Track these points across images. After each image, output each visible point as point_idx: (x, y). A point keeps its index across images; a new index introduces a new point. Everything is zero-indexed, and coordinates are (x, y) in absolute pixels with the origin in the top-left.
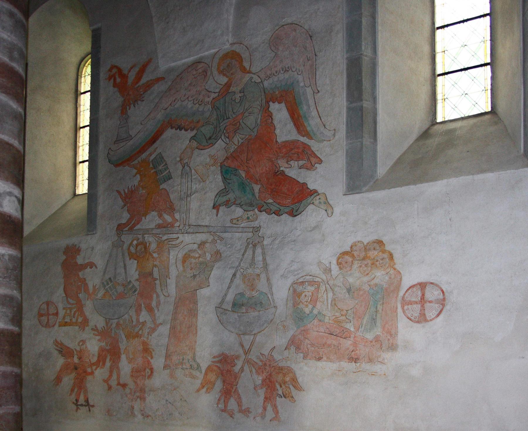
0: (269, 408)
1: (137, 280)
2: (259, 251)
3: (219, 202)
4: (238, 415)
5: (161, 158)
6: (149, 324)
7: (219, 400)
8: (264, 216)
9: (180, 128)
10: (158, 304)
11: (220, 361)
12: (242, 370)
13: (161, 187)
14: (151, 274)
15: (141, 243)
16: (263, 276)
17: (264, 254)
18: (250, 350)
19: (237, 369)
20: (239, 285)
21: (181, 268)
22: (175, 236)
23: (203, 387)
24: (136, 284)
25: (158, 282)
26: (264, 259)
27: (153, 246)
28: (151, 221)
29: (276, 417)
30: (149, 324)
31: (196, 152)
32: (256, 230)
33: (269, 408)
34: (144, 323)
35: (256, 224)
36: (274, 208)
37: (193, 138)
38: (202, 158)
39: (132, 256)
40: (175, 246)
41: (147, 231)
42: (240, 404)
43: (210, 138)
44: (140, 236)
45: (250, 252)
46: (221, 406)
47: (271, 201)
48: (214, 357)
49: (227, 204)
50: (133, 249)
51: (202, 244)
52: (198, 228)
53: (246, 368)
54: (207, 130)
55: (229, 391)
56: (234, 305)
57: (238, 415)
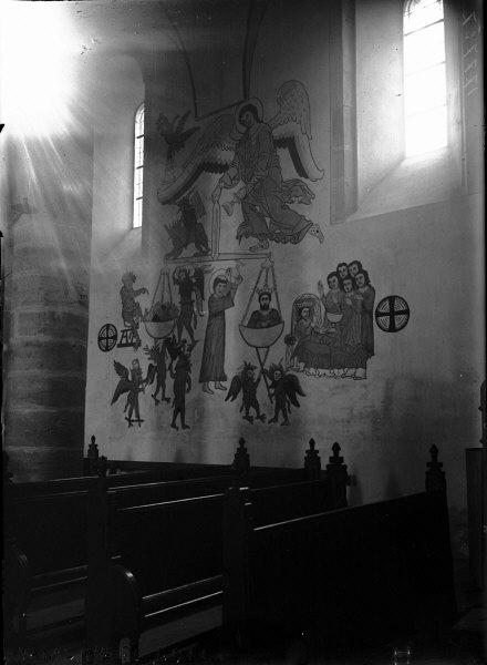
12: (259, 380)
25: (195, 304)
26: (275, 281)
28: (190, 250)
30: (189, 342)
32: (269, 255)
34: (185, 341)
38: (227, 196)
50: (177, 277)
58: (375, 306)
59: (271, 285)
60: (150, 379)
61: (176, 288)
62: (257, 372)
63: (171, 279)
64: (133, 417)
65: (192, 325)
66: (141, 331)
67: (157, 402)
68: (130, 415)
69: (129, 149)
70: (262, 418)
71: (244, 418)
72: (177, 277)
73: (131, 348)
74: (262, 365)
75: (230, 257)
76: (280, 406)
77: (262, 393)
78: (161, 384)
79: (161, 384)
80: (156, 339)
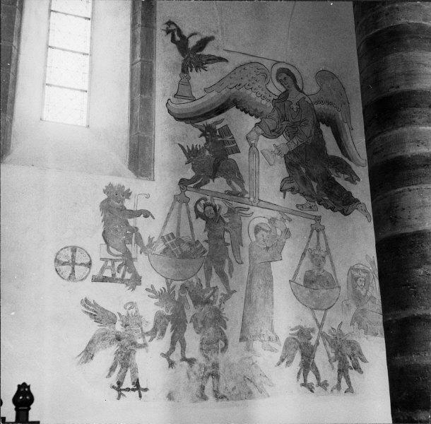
0: (343, 380)
1: (206, 241)
2: (321, 235)
3: (284, 188)
4: (317, 389)
6: (222, 290)
7: (299, 374)
8: (322, 208)
11: (298, 334)
12: (318, 343)
14: (222, 238)
16: (327, 259)
17: (326, 239)
18: (322, 324)
19: (313, 342)
20: (307, 265)
21: (254, 239)
22: (246, 206)
23: (282, 360)
24: (206, 246)
26: (327, 244)
27: (224, 211)
28: (218, 185)
29: (350, 390)
30: (222, 290)
32: (318, 219)
33: (343, 380)
34: (215, 289)
38: (265, 144)
39: (198, 215)
40: (247, 216)
42: (318, 379)
43: (273, 131)
44: (209, 198)
46: (302, 380)
48: (292, 330)
50: (200, 209)
51: (272, 220)
52: (269, 206)
53: (321, 342)
56: (306, 280)
57: (317, 389)
60: (157, 331)
61: (200, 224)
62: (314, 337)
64: (128, 383)
65: (226, 270)
66: (142, 264)
67: (171, 364)
68: (119, 383)
70: (324, 385)
71: (302, 385)
73: (122, 287)
74: (320, 326)
75: (275, 207)
76: (342, 371)
77: (322, 358)
78: (178, 339)
79: (178, 339)
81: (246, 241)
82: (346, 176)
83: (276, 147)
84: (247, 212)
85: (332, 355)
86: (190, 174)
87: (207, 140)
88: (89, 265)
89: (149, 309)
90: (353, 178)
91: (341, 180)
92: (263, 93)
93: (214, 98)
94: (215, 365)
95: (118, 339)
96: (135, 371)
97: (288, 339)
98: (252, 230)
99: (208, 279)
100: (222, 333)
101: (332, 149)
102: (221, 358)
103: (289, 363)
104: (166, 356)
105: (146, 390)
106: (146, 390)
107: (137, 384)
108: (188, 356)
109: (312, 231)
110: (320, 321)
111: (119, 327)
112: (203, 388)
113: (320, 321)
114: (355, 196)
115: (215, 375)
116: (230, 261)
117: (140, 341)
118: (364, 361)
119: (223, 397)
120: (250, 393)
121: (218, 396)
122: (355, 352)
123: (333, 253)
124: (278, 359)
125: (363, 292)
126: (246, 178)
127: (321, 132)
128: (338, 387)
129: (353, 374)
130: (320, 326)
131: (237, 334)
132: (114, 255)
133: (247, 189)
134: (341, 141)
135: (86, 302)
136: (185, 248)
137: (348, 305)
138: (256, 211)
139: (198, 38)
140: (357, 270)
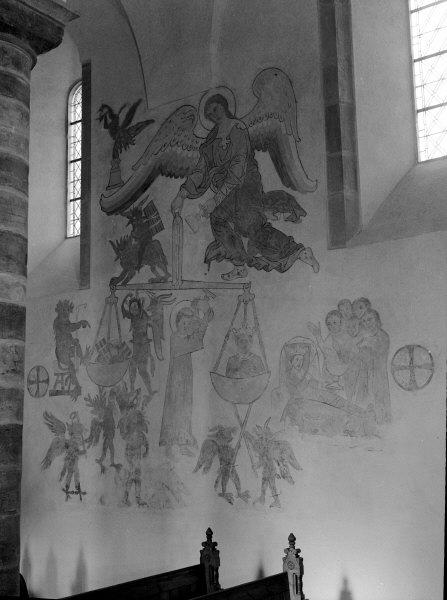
0: (269, 492)
2: (250, 306)
5: (152, 209)
6: (144, 392)
9: (170, 175)
10: (153, 369)
12: (239, 446)
13: (154, 238)
14: (145, 334)
15: (135, 300)
16: (255, 338)
18: (245, 421)
19: (233, 444)
21: (175, 329)
22: (168, 292)
25: (152, 344)
26: (256, 318)
27: (147, 304)
28: (144, 274)
30: (144, 388)
31: (187, 201)
32: (247, 286)
33: (269, 492)
34: (138, 391)
35: (246, 280)
36: (263, 264)
37: (183, 186)
38: (193, 208)
39: (126, 314)
40: (169, 303)
41: (139, 287)
44: (134, 292)
45: (241, 310)
46: (220, 490)
47: (259, 255)
48: (211, 431)
49: (218, 257)
50: (126, 307)
51: (195, 302)
52: (191, 285)
53: (243, 443)
54: (197, 178)
55: (227, 471)
56: (228, 370)
57: (236, 500)
58: (390, 357)
59: (251, 324)
61: (126, 323)
63: (120, 310)
64: (72, 488)
65: (148, 370)
66: (83, 375)
67: (103, 470)
68: (67, 487)
69: (60, 139)
71: (220, 495)
72: (126, 307)
73: (68, 398)
78: (108, 446)
79: (108, 446)
80: (101, 388)
81: (167, 334)
82: (288, 215)
83: (201, 206)
84: (172, 298)
85: (256, 460)
86: (118, 271)
87: (134, 227)
88: (47, 381)
89: (87, 417)
90: (296, 213)
91: (280, 223)
92: (189, 143)
93: (142, 172)
94: (138, 471)
95: (67, 447)
96: (77, 476)
97: (206, 442)
98: (174, 318)
99: (132, 382)
100: (144, 438)
101: (271, 181)
102: (142, 463)
103: (207, 469)
104: (99, 461)
105: (85, 493)
106: (85, 493)
107: (78, 487)
108: (116, 463)
109: (239, 305)
110: (243, 418)
111: (67, 436)
112: (127, 494)
113: (243, 418)
114: (297, 241)
115: (137, 481)
116: (152, 360)
117: (81, 448)
118: (297, 468)
119: (144, 504)
120: (168, 501)
121: (141, 504)
122: (285, 456)
123: (262, 328)
124: (195, 464)
125: (300, 376)
126: (169, 260)
127: (256, 164)
128: (262, 499)
129: (280, 484)
130: (243, 425)
131: (157, 440)
132: (61, 368)
133: (170, 272)
134: (283, 165)
135: (47, 416)
136: (114, 352)
137: (278, 395)
138: (178, 295)
139: (126, 110)
140: (293, 346)
